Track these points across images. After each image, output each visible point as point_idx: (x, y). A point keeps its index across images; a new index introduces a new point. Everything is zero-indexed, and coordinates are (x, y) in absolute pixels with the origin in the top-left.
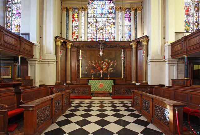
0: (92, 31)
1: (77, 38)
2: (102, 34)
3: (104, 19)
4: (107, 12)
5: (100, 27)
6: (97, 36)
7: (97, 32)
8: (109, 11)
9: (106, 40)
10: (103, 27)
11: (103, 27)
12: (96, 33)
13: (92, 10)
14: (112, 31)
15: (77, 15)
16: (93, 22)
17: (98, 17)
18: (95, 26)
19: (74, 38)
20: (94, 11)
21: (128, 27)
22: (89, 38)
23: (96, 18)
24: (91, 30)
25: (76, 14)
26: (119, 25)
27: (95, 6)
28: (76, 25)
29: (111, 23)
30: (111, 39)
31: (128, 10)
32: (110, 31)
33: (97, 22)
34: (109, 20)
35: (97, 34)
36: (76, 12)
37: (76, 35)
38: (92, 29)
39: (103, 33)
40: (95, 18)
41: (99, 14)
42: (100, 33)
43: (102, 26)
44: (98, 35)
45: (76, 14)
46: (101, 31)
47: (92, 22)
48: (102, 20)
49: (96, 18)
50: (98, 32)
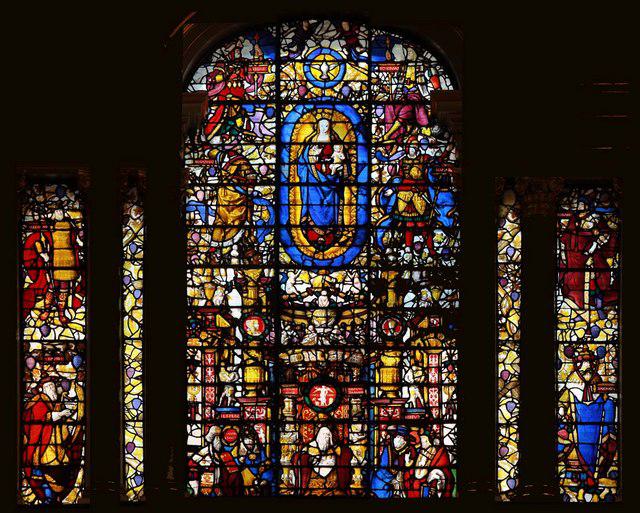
0: (228, 391)
1: (74, 467)
2: (331, 423)
3: (352, 285)
4: (376, 216)
5: (310, 356)
6: (276, 446)
7: (276, 404)
8: (402, 206)
9: (367, 481)
10: (333, 356)
11: (333, 356)
12: (264, 413)
13: (228, 195)
14: (432, 396)
15: (73, 246)
16: (236, 314)
17: (285, 258)
18: (257, 349)
19: (46, 468)
20: (248, 202)
21: (595, 360)
22: (203, 459)
23: (270, 273)
24: (220, 386)
25: (60, 238)
26: (503, 336)
27: (260, 158)
28: (56, 333)
29: (424, 324)
30: (420, 474)
31: (589, 202)
32: (411, 394)
33: (276, 306)
34: (403, 287)
35: (276, 424)
36: (58, 215)
37: (57, 437)
38: (225, 376)
39: (342, 412)
40: (253, 274)
41: (299, 236)
42: (308, 413)
43: (335, 345)
44: (288, 437)
45: (60, 238)
46: (324, 395)
47: (225, 310)
48: (332, 289)
49: (270, 273)
50: (288, 404)
